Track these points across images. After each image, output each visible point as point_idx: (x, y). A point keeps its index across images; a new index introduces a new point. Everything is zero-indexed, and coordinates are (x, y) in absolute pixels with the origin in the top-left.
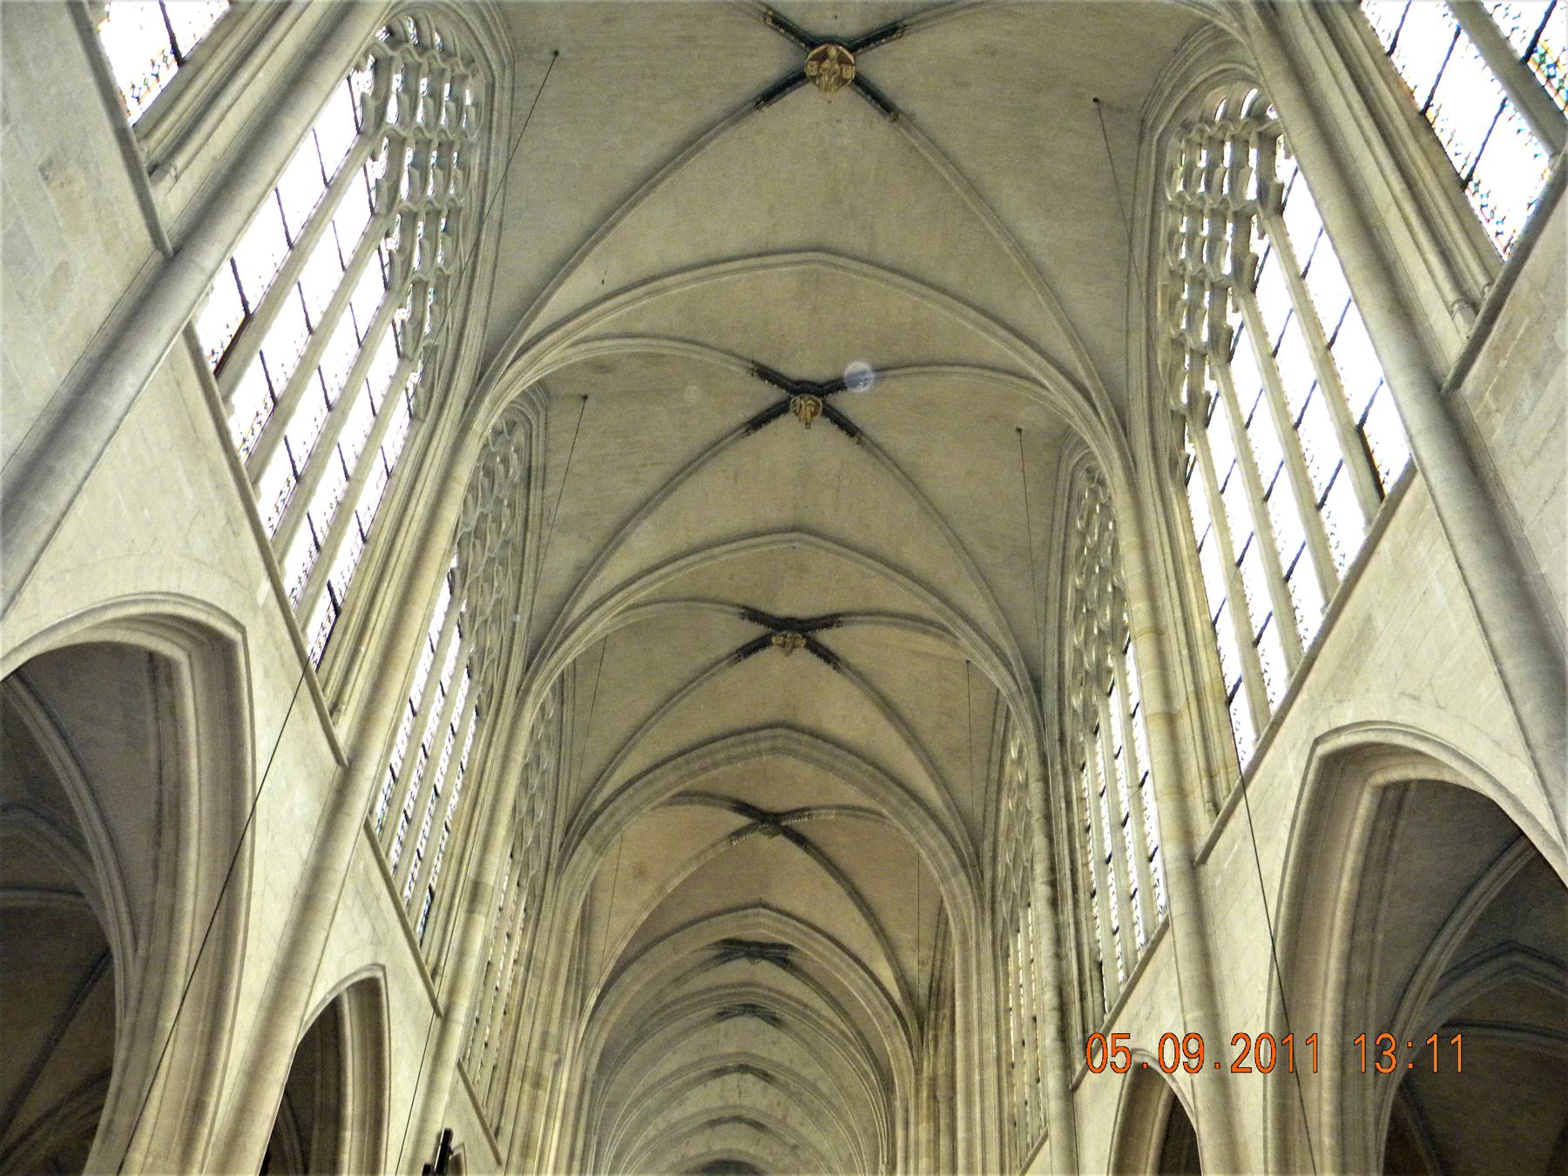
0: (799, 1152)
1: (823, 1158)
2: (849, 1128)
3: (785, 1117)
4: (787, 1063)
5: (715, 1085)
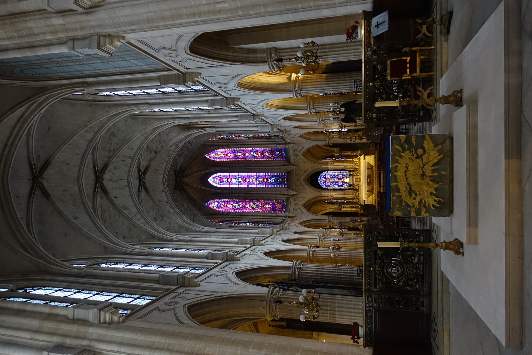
0: (158, 150)
1: (147, 138)
2: (109, 119)
3: (130, 157)
4: (80, 157)
5: (112, 193)
